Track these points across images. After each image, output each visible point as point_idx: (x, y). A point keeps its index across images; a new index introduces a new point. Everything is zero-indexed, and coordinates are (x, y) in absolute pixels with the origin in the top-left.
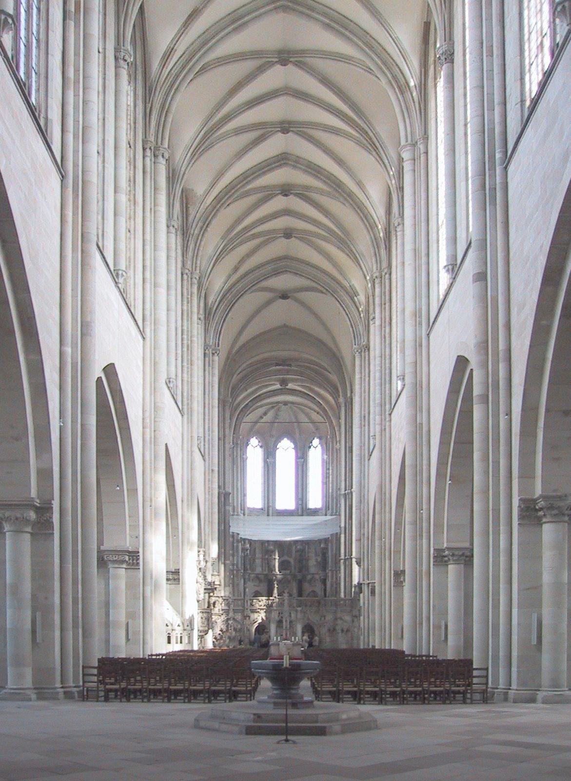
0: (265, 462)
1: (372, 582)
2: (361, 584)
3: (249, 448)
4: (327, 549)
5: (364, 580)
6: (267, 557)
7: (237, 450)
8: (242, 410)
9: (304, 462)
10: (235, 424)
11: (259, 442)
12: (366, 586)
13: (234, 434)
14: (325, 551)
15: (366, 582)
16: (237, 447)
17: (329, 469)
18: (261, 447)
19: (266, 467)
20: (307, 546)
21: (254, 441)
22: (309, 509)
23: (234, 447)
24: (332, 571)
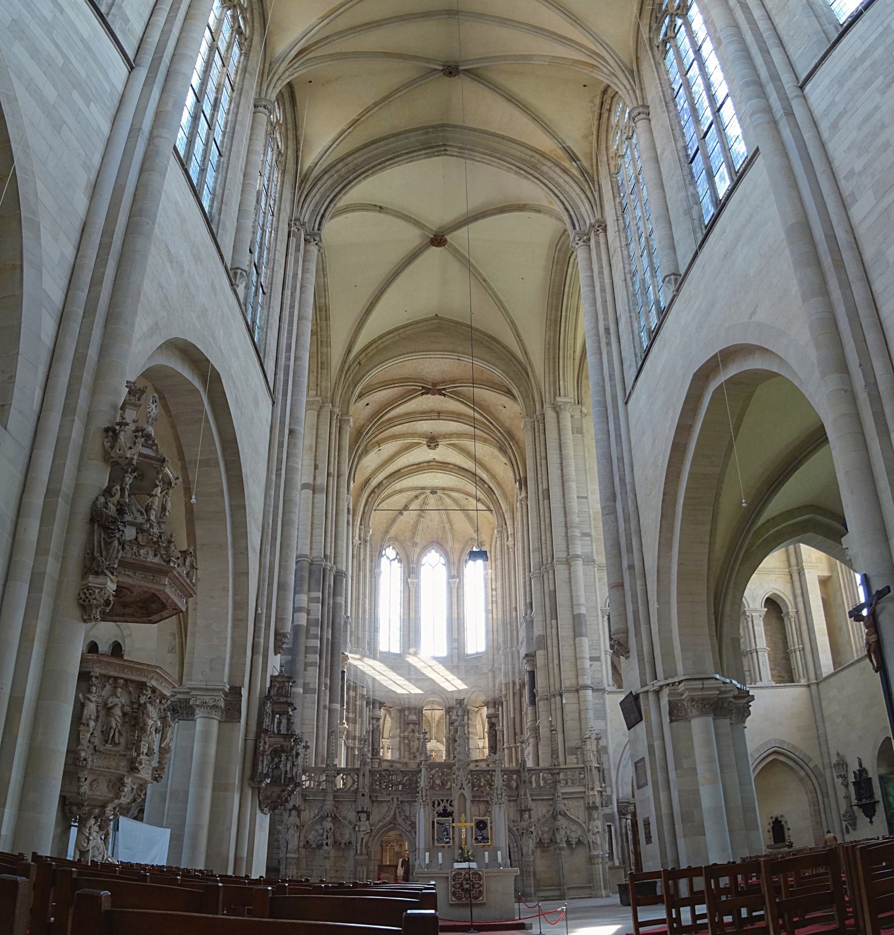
0: (406, 583)
1: (670, 681)
2: (637, 697)
3: (384, 560)
4: (497, 716)
5: (644, 684)
6: (406, 734)
7: (365, 550)
8: (373, 491)
9: (459, 584)
10: (364, 512)
11: (397, 554)
12: (651, 697)
13: (361, 524)
14: (493, 720)
15: (652, 686)
16: (366, 546)
17: (496, 590)
18: (400, 561)
19: (407, 588)
21: (390, 552)
22: (468, 655)
24: (510, 748)
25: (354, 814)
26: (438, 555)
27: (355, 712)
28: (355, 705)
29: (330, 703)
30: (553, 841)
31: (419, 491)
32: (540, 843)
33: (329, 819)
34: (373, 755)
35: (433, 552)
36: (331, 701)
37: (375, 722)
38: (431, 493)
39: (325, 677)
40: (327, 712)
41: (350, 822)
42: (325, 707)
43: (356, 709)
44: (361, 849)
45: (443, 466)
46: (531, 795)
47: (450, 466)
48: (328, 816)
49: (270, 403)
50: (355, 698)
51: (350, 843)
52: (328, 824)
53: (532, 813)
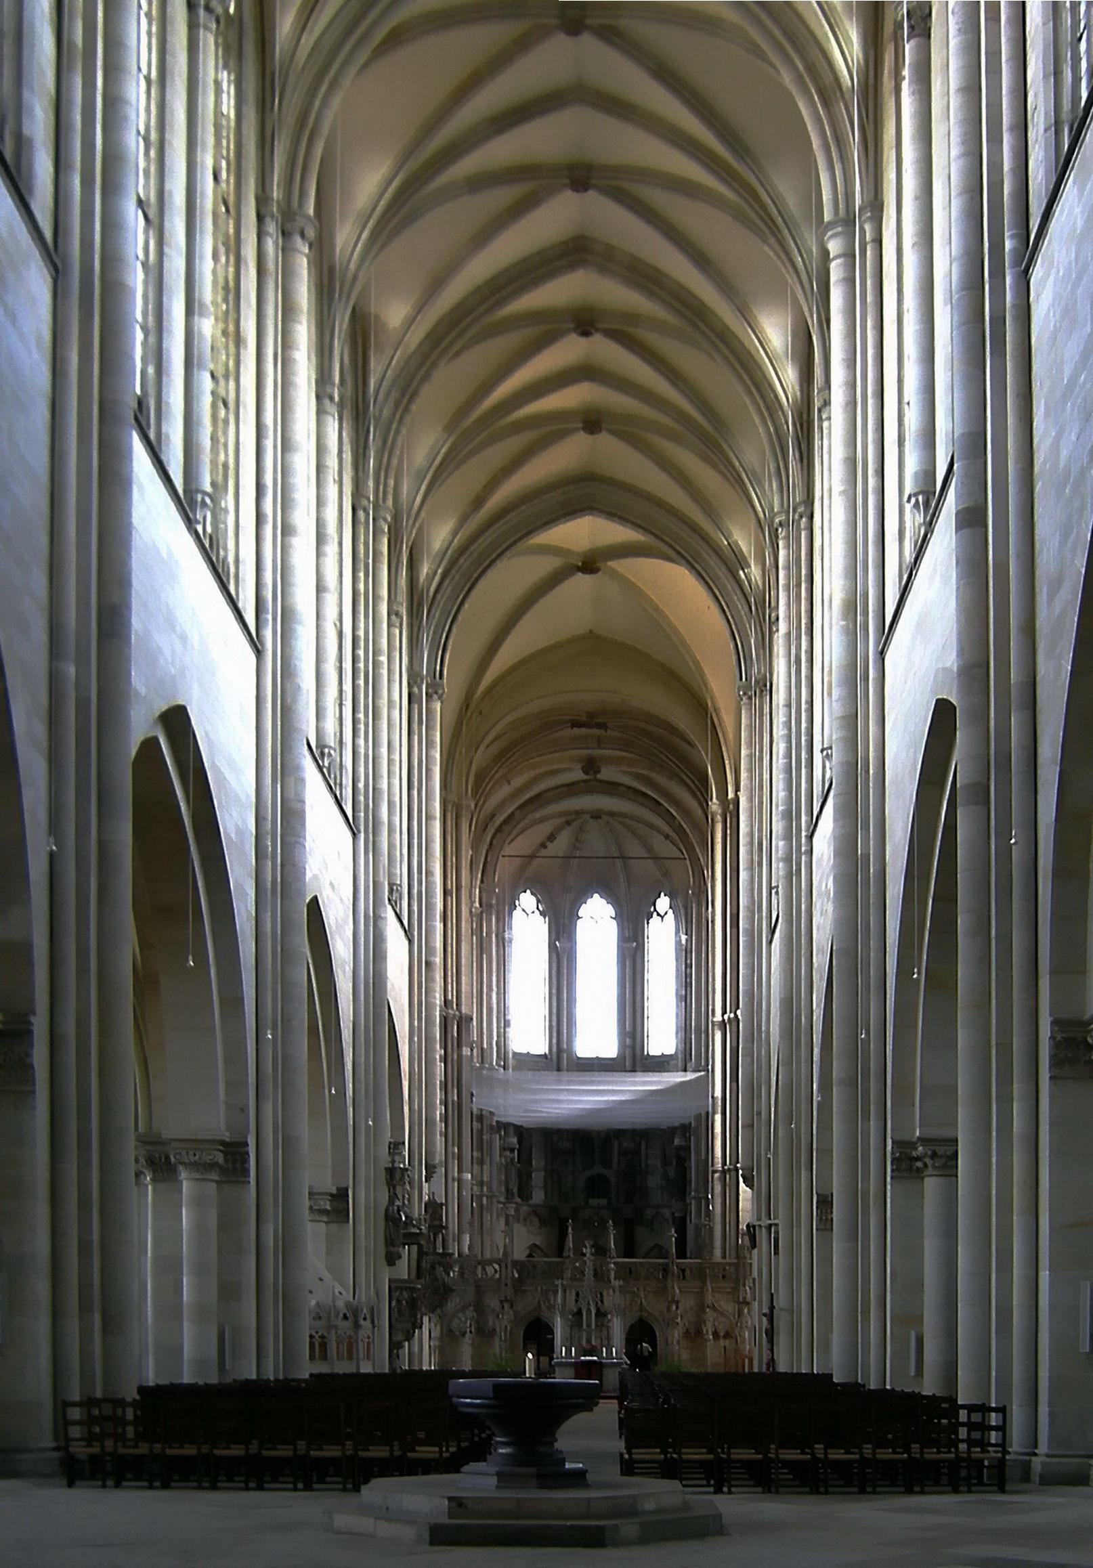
2: (754, 1227)
9: (636, 949)
14: (682, 1153)
19: (555, 959)
20: (643, 1143)
23: (482, 912)
25: (498, 1304)
26: (604, 901)
27: (481, 1150)
28: (482, 1140)
29: (458, 1172)
30: (699, 1333)
31: (574, 816)
32: (687, 1333)
33: (471, 1308)
34: (507, 1198)
35: (596, 896)
36: (460, 1171)
37: (508, 1153)
38: (592, 817)
39: (453, 1145)
40: (456, 1184)
41: (493, 1310)
42: (453, 1179)
43: (482, 1144)
44: (505, 1336)
45: (612, 788)
46: (679, 1288)
47: (621, 788)
48: (470, 1305)
49: (407, 942)
50: (481, 1132)
51: (494, 1329)
52: (471, 1312)
53: (680, 1304)
